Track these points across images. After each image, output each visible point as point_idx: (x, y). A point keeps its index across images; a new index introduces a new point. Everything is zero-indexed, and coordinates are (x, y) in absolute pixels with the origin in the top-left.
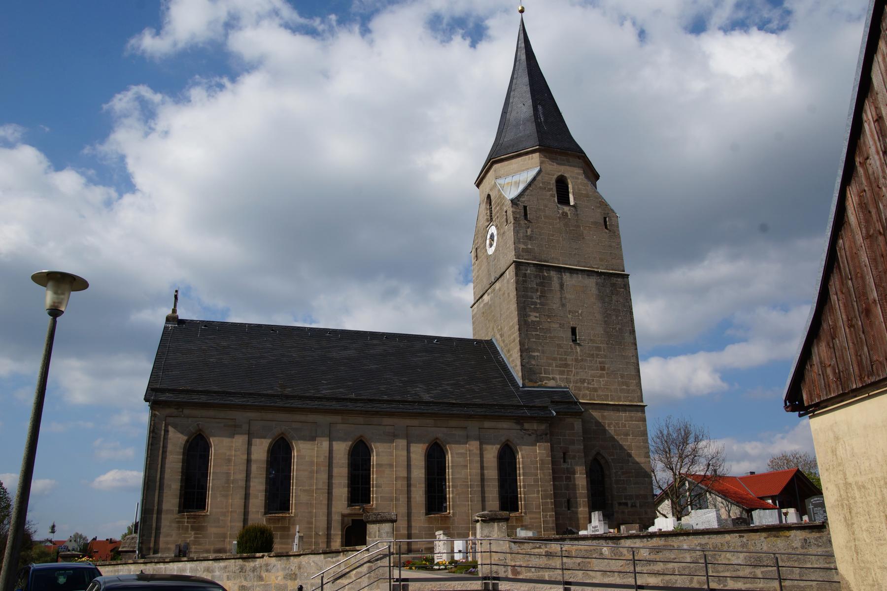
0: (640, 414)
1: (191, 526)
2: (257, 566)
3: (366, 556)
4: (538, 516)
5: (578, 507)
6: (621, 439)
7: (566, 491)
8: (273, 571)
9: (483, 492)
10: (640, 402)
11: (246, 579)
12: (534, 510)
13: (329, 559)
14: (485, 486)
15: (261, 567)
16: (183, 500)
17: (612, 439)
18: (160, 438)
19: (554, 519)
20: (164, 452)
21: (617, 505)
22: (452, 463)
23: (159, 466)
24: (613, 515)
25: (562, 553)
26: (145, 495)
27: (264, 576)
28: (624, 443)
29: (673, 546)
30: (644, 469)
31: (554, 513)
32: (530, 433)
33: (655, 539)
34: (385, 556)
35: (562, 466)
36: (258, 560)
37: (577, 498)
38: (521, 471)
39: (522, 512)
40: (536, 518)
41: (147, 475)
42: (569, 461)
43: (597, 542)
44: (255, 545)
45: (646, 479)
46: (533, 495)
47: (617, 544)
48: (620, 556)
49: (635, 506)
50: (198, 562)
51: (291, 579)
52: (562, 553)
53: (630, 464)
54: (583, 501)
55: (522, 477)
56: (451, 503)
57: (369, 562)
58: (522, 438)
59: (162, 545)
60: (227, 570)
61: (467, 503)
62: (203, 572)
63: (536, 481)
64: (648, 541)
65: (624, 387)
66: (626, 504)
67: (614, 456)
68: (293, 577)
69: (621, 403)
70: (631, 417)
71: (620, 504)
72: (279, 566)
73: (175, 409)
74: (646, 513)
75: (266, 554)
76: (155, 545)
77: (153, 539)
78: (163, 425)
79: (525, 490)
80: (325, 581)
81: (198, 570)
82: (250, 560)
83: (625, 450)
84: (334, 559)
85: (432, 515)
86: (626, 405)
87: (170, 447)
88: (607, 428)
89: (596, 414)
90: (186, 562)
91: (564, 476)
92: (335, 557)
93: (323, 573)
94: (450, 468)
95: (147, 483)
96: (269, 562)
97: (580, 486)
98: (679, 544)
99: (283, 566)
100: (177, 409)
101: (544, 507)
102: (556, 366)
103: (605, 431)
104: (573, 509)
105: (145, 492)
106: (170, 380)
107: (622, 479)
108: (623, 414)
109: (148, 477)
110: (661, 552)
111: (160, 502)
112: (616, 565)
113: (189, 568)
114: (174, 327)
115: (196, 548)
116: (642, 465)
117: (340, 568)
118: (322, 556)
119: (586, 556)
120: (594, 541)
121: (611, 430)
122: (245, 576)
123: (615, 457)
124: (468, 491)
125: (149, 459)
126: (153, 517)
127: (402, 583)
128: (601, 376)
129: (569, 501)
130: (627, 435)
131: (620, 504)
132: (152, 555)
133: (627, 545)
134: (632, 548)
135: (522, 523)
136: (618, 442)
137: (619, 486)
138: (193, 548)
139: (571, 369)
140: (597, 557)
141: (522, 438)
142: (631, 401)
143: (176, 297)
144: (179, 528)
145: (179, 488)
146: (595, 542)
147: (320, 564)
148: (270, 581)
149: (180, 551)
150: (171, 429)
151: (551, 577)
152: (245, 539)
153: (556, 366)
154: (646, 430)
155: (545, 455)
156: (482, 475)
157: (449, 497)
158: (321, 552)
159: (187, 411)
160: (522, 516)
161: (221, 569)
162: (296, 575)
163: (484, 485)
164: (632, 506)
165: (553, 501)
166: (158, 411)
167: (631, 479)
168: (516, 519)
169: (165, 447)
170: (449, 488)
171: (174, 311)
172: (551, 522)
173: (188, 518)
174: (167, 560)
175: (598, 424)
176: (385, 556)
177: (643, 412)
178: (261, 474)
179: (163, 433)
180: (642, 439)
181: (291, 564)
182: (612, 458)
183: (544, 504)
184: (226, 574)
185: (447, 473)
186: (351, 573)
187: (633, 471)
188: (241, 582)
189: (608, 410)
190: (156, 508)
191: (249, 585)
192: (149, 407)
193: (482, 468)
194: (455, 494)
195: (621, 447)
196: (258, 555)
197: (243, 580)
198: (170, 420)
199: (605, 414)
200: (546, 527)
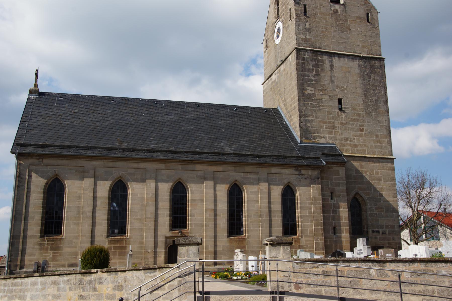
0: (390, 165)
1: (50, 247)
2: (93, 279)
3: (177, 272)
4: (311, 239)
5: (342, 233)
6: (375, 183)
7: (332, 221)
8: (104, 284)
9: (270, 220)
10: (391, 156)
11: (83, 290)
12: (308, 235)
13: (148, 274)
15: (95, 280)
16: (44, 228)
17: (368, 183)
18: (25, 181)
19: (324, 241)
20: (28, 192)
21: (371, 233)
22: (247, 199)
23: (25, 203)
25: (337, 273)
26: (13, 225)
27: (98, 287)
28: (377, 186)
29: (433, 271)
30: (392, 206)
31: (323, 237)
32: (306, 177)
33: (416, 264)
34: (190, 273)
35: (330, 202)
36: (93, 274)
37: (341, 226)
38: (299, 206)
39: (299, 236)
40: (310, 241)
41: (14, 209)
42: (335, 198)
43: (365, 264)
44: (95, 262)
45: (394, 214)
46: (308, 223)
47: (383, 267)
48: (385, 277)
49: (385, 233)
50: (47, 277)
51: (118, 290)
52: (337, 273)
53: (382, 202)
54: (346, 229)
55: (299, 210)
56: (246, 229)
57: (179, 277)
58: (300, 181)
59: (27, 262)
60: (69, 283)
61: (258, 229)
62: (51, 284)
63: (310, 213)
64: (410, 265)
65: (378, 144)
66: (378, 232)
67: (369, 196)
68: (120, 288)
69: (375, 156)
70: (383, 167)
71: (373, 232)
72: (109, 280)
73: (37, 159)
74: (394, 239)
75: (99, 270)
76: (21, 262)
77: (19, 258)
78: (27, 171)
79: (302, 219)
80: (142, 293)
81: (47, 283)
82: (87, 275)
83: (379, 192)
84: (152, 274)
86: (379, 158)
87: (33, 188)
88: (364, 175)
89: (356, 164)
90: (38, 277)
92: (152, 273)
93: (140, 287)
95: (15, 215)
96: (101, 277)
97: (343, 217)
98: (438, 269)
99: (112, 279)
100: (38, 159)
101: (316, 232)
102: (326, 128)
103: (362, 177)
104: (338, 234)
105: (13, 222)
106: (33, 137)
107: (375, 213)
108: (376, 165)
109: (16, 211)
110: (421, 275)
111: (25, 230)
112: (381, 285)
113: (40, 282)
114: (36, 98)
115: (54, 264)
116: (391, 203)
117: (156, 281)
118: (143, 271)
119: (356, 276)
120: (363, 264)
121: (367, 176)
122: (83, 287)
123: (370, 197)
124: (259, 219)
125: (16, 197)
126: (19, 241)
127: (205, 296)
128: (360, 136)
129: (334, 228)
130: (379, 180)
131: (373, 232)
132: (18, 270)
133: (391, 268)
134: (398, 271)
136: (372, 185)
137: (373, 218)
138: (51, 264)
140: (366, 277)
141: (300, 181)
142: (383, 155)
143: (37, 75)
144: (40, 249)
145: (41, 218)
146: (364, 265)
147: (141, 278)
148: (102, 291)
149: (38, 267)
150: (33, 174)
151: (327, 292)
152: (87, 257)
153: (326, 128)
154: (395, 177)
155: (317, 194)
156: (270, 208)
158: (142, 268)
159: (46, 161)
160: (299, 239)
161: (64, 282)
162: (122, 287)
163: (271, 215)
164: (383, 233)
165: (323, 228)
166: (23, 161)
167: (382, 213)
169: (29, 188)
170: (245, 218)
171: (36, 85)
172: (321, 244)
173: (48, 241)
174: (23, 276)
175: (357, 171)
176: (190, 273)
177: (393, 163)
178: (104, 207)
179: (27, 177)
180: (392, 183)
181: (119, 278)
182: (368, 197)
184: (68, 286)
186: (165, 286)
187: (384, 207)
188: (80, 292)
189: (365, 161)
190: (22, 234)
191: (86, 295)
192: (16, 158)
193: (270, 203)
194: (249, 222)
195: (375, 189)
196: (93, 271)
197: (82, 291)
198: (32, 167)
199: (363, 164)
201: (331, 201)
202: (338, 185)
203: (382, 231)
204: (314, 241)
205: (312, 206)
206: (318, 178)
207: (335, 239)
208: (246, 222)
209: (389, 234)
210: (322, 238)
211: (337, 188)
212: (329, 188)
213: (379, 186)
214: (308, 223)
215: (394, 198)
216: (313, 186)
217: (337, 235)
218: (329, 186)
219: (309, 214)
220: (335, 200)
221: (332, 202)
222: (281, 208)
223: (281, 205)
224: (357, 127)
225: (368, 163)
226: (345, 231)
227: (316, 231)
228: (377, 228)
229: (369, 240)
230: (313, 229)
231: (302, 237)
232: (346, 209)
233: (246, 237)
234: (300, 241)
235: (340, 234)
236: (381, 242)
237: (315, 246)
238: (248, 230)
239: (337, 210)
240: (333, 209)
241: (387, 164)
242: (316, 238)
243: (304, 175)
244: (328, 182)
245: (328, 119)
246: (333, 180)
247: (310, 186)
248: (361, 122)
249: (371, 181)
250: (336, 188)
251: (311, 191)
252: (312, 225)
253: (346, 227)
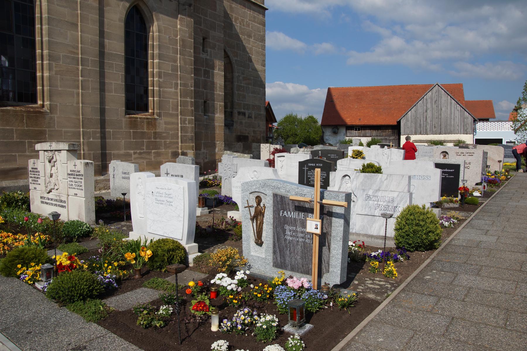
0: (261, 16)
4: (173, 120)
5: (215, 113)
6: (245, 39)
7: (203, 90)
9: (102, 75)
10: (262, 4)
12: (171, 112)
14: (105, 64)
19: (194, 125)
22: (49, 13)
24: (232, 125)
28: (247, 45)
30: (260, 77)
31: (193, 118)
35: (201, 56)
37: (214, 101)
38: (156, 52)
39: (153, 114)
40: (173, 123)
42: (209, 50)
45: (261, 89)
46: (171, 90)
53: (250, 70)
54: (220, 106)
55: (156, 61)
56: (46, 88)
61: (75, 91)
63: (175, 69)
66: (244, 114)
70: (255, 17)
71: (239, 113)
79: (161, 80)
83: (248, 53)
85: (9, 108)
88: (234, 23)
91: (203, 69)
94: (44, 22)
97: (218, 85)
104: (210, 114)
107: (242, 85)
124: (78, 69)
129: (205, 102)
130: (250, 36)
135: (155, 130)
137: (240, 93)
154: (265, 36)
156: (102, 46)
157: (43, 76)
160: (155, 119)
163: (103, 63)
164: (249, 117)
165: (193, 100)
167: (250, 86)
168: (148, 124)
170: (42, 60)
172: (190, 130)
177: (264, 15)
180: (261, 45)
182: (236, 59)
183: (183, 104)
185: (37, 31)
187: (252, 78)
193: (102, 34)
194: (54, 73)
195: (244, 49)
199: (233, 6)
200: (185, 136)
203: (248, 114)
204: (180, 125)
205: (179, 56)
207: (205, 123)
208: (45, 72)
209: (255, 118)
210: (192, 119)
213: (248, 45)
214: (170, 88)
215: (263, 67)
216: (181, 18)
217: (208, 116)
219: (172, 70)
220: (209, 52)
222: (123, 51)
223: (123, 44)
225: (239, 5)
226: (220, 109)
227: (184, 107)
228: (244, 109)
229: (234, 125)
230: (178, 101)
231: (159, 115)
232: (222, 71)
233: (45, 109)
234: (157, 124)
235: (213, 115)
236: (246, 130)
237: (180, 134)
238: (50, 91)
239: (211, 70)
240: (204, 68)
241: (258, 15)
242: (182, 119)
244: (201, 18)
247: (177, 18)
249: (240, 36)
250: (210, 31)
251: (179, 27)
252: (177, 93)
253: (221, 103)
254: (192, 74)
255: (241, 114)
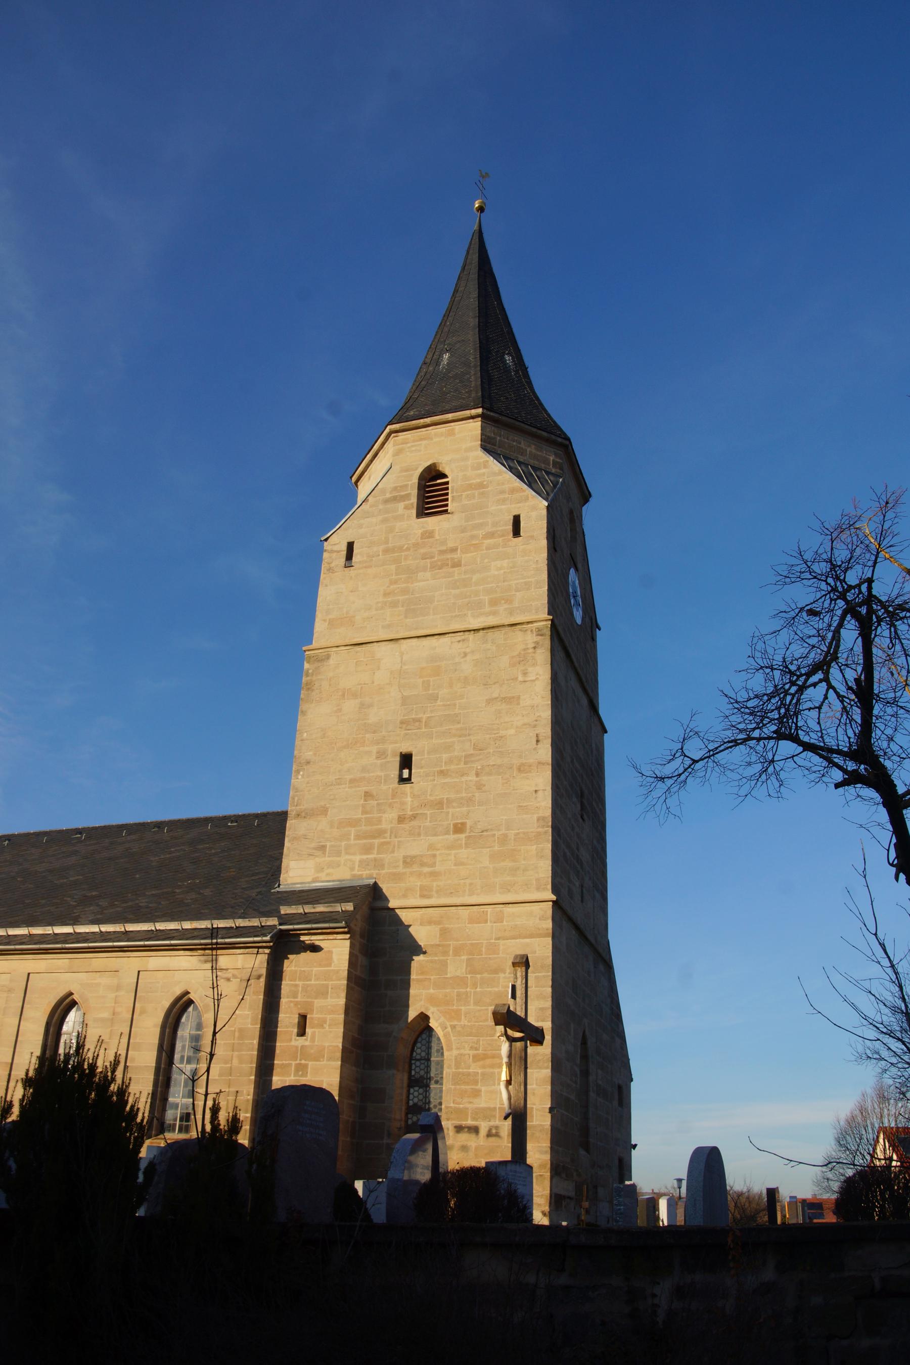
49: (497, 1135)
66: (475, 1130)
67: (459, 1020)
71: (459, 1129)
91: (294, 1063)
102: (358, 837)
131: (459, 1129)
139: (388, 840)
153: (358, 837)
155: (249, 1020)
164: (489, 1135)
182: (455, 1023)
201: (295, 1040)
202: (323, 993)
203: (487, 1129)
206: (259, 977)
211: (318, 1003)
212: (296, 1004)
218: (297, 997)
221: (300, 1041)
224: (446, 823)
228: (474, 1119)
240: (298, 1062)
243: (227, 969)
244: (296, 986)
245: (364, 812)
246: (310, 980)
248: (460, 807)
250: (316, 1001)
254: (251, 1076)
255: (466, 1130)
